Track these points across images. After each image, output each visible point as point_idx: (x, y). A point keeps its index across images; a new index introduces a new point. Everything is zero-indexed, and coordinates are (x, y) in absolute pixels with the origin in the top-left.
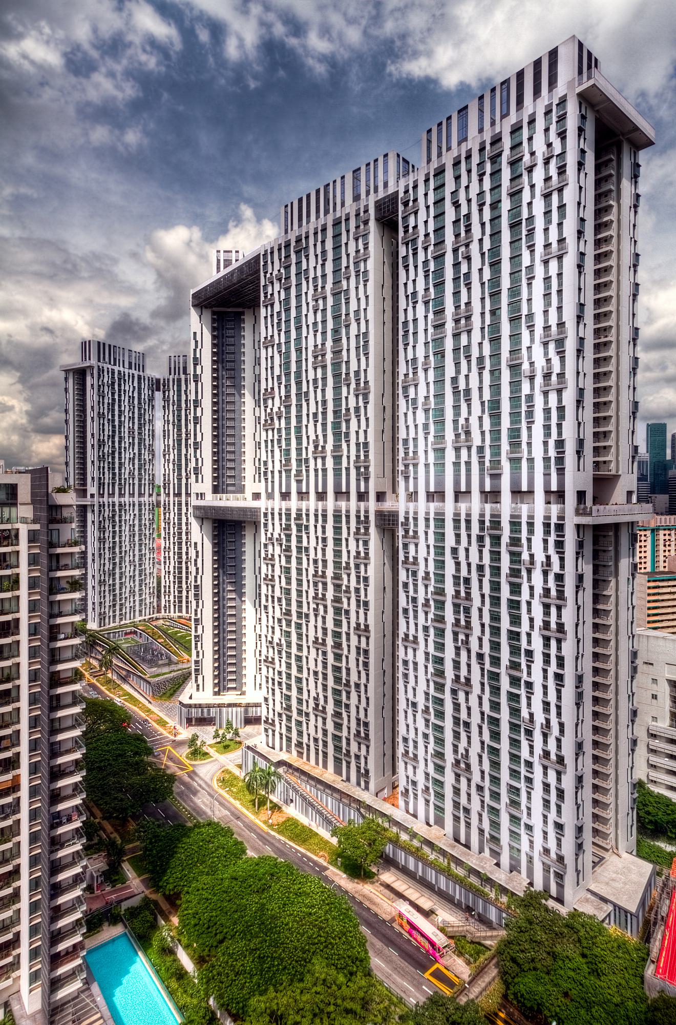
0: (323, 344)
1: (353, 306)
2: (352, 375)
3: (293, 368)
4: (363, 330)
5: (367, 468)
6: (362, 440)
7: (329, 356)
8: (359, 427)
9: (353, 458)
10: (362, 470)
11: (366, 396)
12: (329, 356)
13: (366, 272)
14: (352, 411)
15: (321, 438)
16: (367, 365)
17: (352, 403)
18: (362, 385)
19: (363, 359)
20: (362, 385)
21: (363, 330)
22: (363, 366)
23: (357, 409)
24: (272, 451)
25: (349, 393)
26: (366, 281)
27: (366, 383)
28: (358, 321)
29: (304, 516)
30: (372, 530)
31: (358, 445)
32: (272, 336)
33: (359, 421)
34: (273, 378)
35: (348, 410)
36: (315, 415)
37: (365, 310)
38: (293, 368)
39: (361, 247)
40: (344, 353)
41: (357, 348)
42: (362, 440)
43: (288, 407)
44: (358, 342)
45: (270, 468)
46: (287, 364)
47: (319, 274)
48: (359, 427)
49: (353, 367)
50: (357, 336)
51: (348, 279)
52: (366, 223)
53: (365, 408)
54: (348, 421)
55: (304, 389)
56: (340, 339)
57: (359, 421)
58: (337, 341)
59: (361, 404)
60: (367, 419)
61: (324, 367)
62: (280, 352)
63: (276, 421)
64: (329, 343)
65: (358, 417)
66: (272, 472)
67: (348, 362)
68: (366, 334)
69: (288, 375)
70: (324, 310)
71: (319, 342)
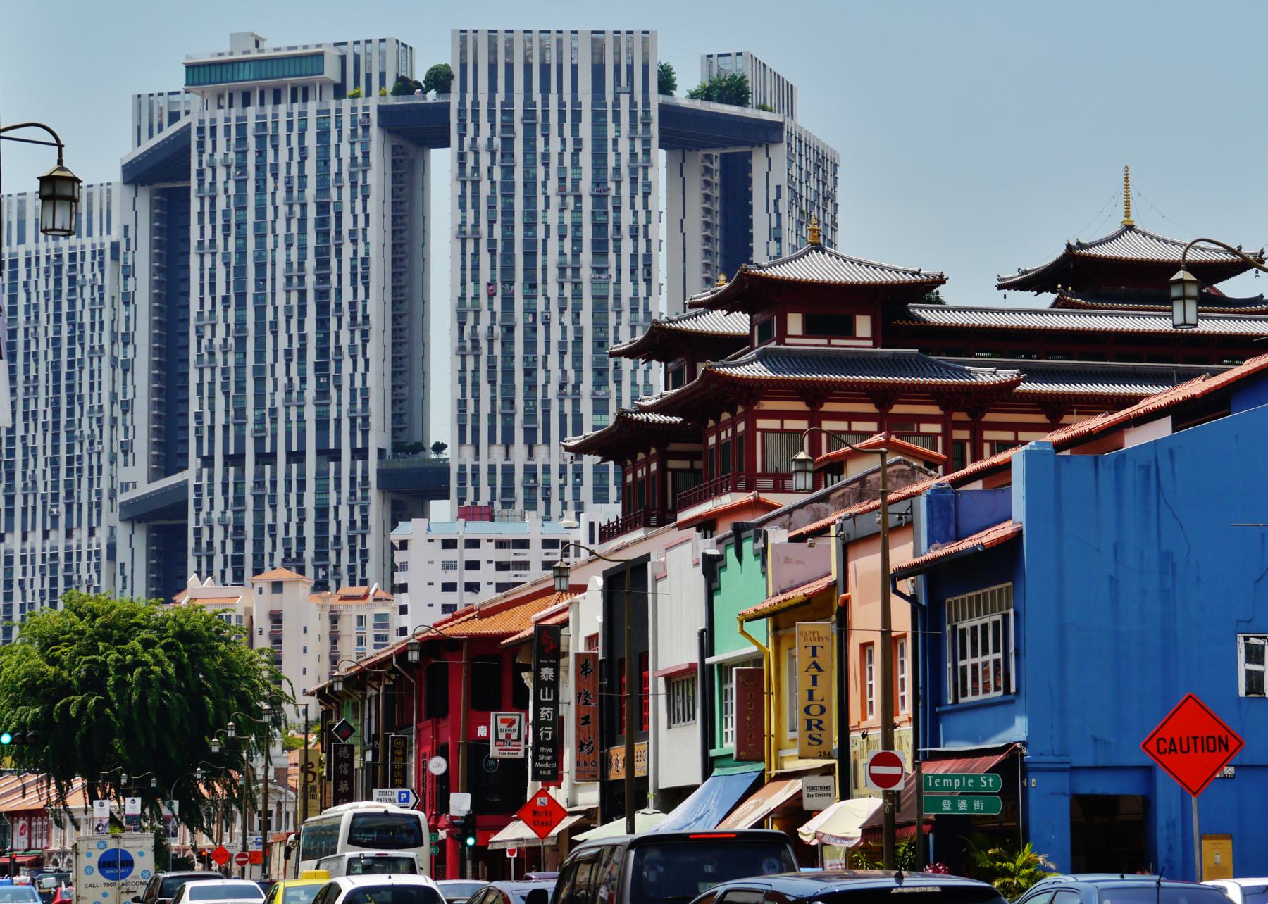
0: (301, 265)
1: (347, 223)
2: (345, 306)
3: (251, 288)
6: (358, 384)
7: (310, 280)
8: (355, 369)
11: (365, 334)
13: (365, 188)
14: (345, 350)
15: (296, 381)
16: (367, 296)
18: (360, 319)
20: (360, 319)
21: (361, 254)
23: (352, 348)
25: (340, 326)
26: (365, 198)
28: (354, 242)
29: (268, 484)
30: (373, 493)
31: (353, 390)
32: (213, 241)
34: (214, 299)
35: (338, 348)
36: (288, 353)
37: (364, 230)
38: (251, 288)
39: (359, 154)
40: (334, 278)
43: (241, 342)
44: (354, 267)
45: (207, 421)
46: (241, 284)
48: (355, 369)
49: (347, 296)
50: (354, 259)
51: (340, 188)
52: (366, 128)
53: (364, 347)
54: (338, 362)
56: (328, 262)
58: (323, 263)
59: (358, 341)
60: (367, 362)
62: (227, 264)
63: (219, 357)
65: (354, 358)
66: (212, 429)
67: (339, 291)
68: (365, 261)
69: (241, 298)
71: (294, 258)
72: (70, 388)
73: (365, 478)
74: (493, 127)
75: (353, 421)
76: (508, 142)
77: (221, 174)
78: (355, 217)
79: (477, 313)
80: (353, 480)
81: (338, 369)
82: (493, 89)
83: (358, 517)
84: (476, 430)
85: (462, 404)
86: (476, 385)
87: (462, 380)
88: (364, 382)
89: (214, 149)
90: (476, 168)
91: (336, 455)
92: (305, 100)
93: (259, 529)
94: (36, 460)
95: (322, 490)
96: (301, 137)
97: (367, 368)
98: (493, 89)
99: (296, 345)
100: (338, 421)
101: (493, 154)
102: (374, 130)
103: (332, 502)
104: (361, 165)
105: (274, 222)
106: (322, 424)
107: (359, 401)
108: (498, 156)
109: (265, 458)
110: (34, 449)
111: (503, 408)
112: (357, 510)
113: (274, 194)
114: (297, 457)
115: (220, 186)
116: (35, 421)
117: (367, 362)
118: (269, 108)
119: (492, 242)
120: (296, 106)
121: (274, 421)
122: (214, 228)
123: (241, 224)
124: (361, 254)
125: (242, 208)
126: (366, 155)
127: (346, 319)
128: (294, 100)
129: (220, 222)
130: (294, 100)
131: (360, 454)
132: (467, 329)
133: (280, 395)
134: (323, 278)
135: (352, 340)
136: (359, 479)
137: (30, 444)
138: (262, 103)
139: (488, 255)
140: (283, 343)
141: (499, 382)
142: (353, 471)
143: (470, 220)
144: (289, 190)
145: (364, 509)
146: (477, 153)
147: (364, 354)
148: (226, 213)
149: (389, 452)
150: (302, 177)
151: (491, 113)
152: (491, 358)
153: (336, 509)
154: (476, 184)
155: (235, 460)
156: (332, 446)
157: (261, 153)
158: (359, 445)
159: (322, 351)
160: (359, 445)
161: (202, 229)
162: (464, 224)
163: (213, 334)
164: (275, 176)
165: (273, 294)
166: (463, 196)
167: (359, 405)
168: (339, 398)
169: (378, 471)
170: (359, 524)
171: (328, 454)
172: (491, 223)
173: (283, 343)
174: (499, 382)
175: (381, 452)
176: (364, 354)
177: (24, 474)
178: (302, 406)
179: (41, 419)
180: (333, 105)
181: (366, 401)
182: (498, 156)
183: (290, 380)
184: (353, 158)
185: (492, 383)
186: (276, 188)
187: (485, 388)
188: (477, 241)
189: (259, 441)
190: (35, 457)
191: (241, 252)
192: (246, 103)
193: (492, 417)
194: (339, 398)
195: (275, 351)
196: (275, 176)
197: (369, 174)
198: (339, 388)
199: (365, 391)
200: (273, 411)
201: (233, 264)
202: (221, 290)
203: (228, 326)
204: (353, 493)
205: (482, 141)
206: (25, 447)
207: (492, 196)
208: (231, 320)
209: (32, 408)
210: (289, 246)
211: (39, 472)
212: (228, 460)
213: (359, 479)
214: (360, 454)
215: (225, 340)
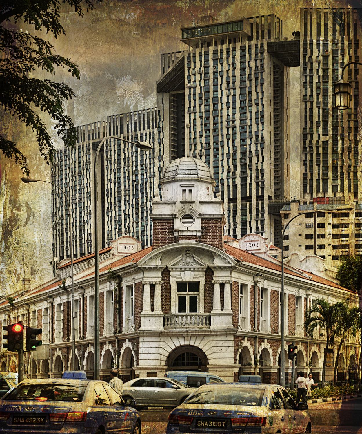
1: (254, 96)
4: (260, 110)
5: (263, 183)
6: (259, 168)
7: (238, 123)
8: (258, 161)
10: (260, 183)
12: (238, 123)
15: (232, 167)
26: (262, 84)
27: (262, 138)
28: (257, 104)
30: (266, 215)
31: (257, 170)
33: (258, 158)
35: (250, 152)
36: (228, 154)
40: (248, 121)
41: (257, 118)
42: (259, 168)
43: (208, 150)
47: (230, 75)
48: (258, 161)
49: (254, 129)
52: (262, 53)
55: (220, 139)
57: (258, 158)
60: (263, 157)
62: (201, 117)
64: (238, 116)
70: (234, 96)
71: (231, 113)
72: (142, 189)
73: (263, 208)
74: (319, 50)
75: (257, 184)
76: (326, 58)
77: (198, 77)
78: (257, 93)
79: (312, 135)
80: (257, 209)
81: (250, 161)
82: (319, 34)
83: (259, 225)
84: (311, 186)
85: (305, 174)
86: (311, 167)
87: (305, 164)
88: (262, 166)
89: (195, 67)
90: (311, 70)
91: (250, 199)
92: (235, 42)
94: (129, 219)
95: (243, 214)
97: (263, 160)
98: (319, 34)
99: (232, 151)
100: (250, 184)
101: (319, 63)
102: (265, 54)
103: (248, 219)
104: (259, 71)
105: (221, 97)
106: (243, 186)
107: (260, 175)
108: (321, 64)
110: (129, 215)
111: (323, 176)
112: (259, 222)
113: (221, 85)
116: (129, 204)
117: (263, 157)
118: (219, 48)
119: (318, 102)
120: (231, 45)
122: (195, 101)
123: (207, 100)
125: (207, 92)
126: (262, 65)
127: (254, 139)
128: (230, 43)
129: (197, 98)
130: (230, 43)
131: (260, 198)
132: (307, 142)
133: (225, 174)
134: (243, 120)
135: (256, 148)
136: (260, 209)
137: (127, 213)
138: (216, 45)
139: (317, 109)
140: (226, 151)
141: (322, 165)
142: (257, 204)
143: (309, 93)
145: (262, 222)
146: (312, 63)
147: (262, 154)
148: (201, 94)
149: (273, 198)
150: (234, 76)
151: (318, 45)
152: (318, 155)
153: (250, 222)
154: (311, 77)
156: (248, 195)
157: (215, 66)
158: (260, 194)
159: (243, 153)
160: (260, 194)
161: (190, 101)
162: (305, 95)
163: (195, 149)
164: (222, 77)
165: (221, 129)
166: (305, 83)
167: (260, 177)
168: (251, 174)
169: (268, 205)
170: (260, 228)
171: (246, 199)
172: (318, 95)
173: (226, 151)
174: (322, 165)
175: (269, 197)
176: (262, 154)
177: (125, 224)
178: (235, 178)
179: (131, 203)
180: (247, 44)
181: (262, 176)
182: (321, 64)
183: (229, 167)
185: (319, 166)
186: (222, 82)
187: (315, 168)
188: (312, 103)
190: (129, 218)
191: (207, 111)
192: (209, 45)
193: (318, 180)
194: (251, 174)
195: (223, 154)
196: (222, 77)
197: (264, 73)
198: (251, 170)
199: (262, 170)
201: (204, 117)
203: (202, 144)
204: (257, 215)
205: (314, 57)
206: (125, 214)
207: (319, 82)
208: (203, 142)
209: (127, 199)
210: (228, 108)
211: (131, 224)
213: (260, 209)
214: (260, 198)
215: (201, 151)
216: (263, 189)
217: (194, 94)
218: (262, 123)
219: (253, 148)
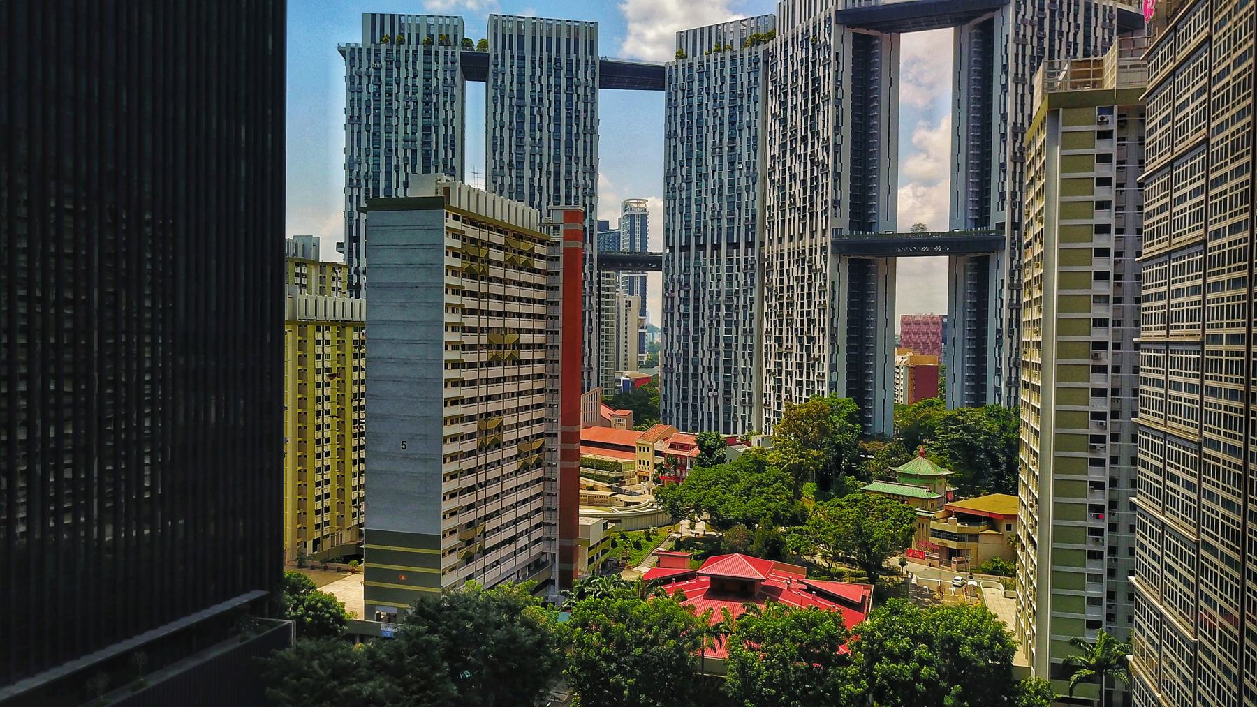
5: (753, 226)
6: (750, 207)
9: (743, 219)
17: (743, 183)
19: (752, 153)
21: (753, 134)
22: (752, 159)
23: (747, 187)
24: (674, 214)
28: (749, 128)
39: (752, 79)
42: (750, 207)
43: (689, 184)
59: (750, 183)
61: (721, 157)
63: (678, 193)
68: (755, 137)
91: (737, 246)
93: (696, 284)
96: (722, 71)
109: (701, 247)
114: (716, 247)
115: (679, 101)
121: (705, 227)
124: (753, 134)
129: (679, 121)
133: (709, 213)
144: (715, 101)
148: (682, 115)
155: (685, 248)
159: (731, 189)
184: (750, 82)
189: (698, 238)
200: (705, 222)
202: (679, 158)
212: (682, 248)
216: (753, 234)
217: (676, 115)
218: (755, 151)
219: (743, 183)
